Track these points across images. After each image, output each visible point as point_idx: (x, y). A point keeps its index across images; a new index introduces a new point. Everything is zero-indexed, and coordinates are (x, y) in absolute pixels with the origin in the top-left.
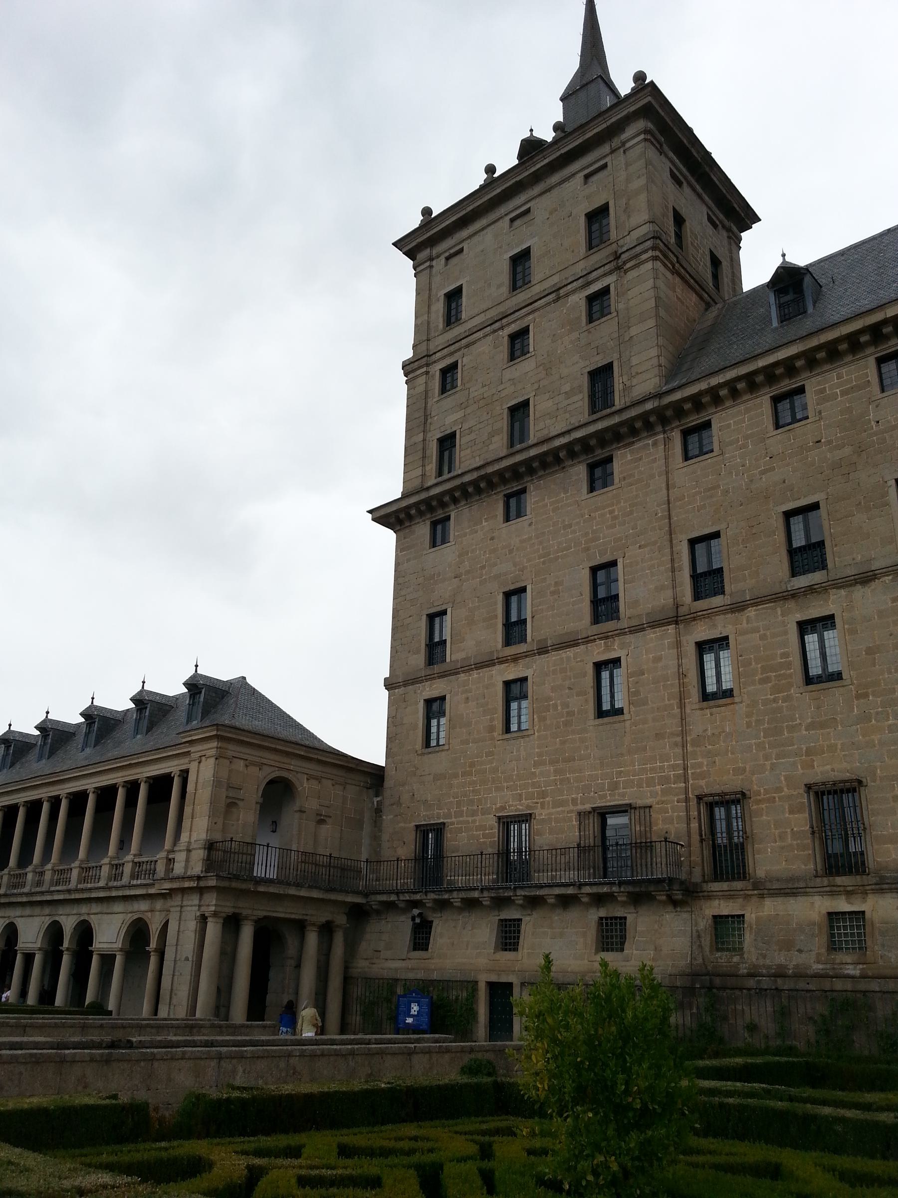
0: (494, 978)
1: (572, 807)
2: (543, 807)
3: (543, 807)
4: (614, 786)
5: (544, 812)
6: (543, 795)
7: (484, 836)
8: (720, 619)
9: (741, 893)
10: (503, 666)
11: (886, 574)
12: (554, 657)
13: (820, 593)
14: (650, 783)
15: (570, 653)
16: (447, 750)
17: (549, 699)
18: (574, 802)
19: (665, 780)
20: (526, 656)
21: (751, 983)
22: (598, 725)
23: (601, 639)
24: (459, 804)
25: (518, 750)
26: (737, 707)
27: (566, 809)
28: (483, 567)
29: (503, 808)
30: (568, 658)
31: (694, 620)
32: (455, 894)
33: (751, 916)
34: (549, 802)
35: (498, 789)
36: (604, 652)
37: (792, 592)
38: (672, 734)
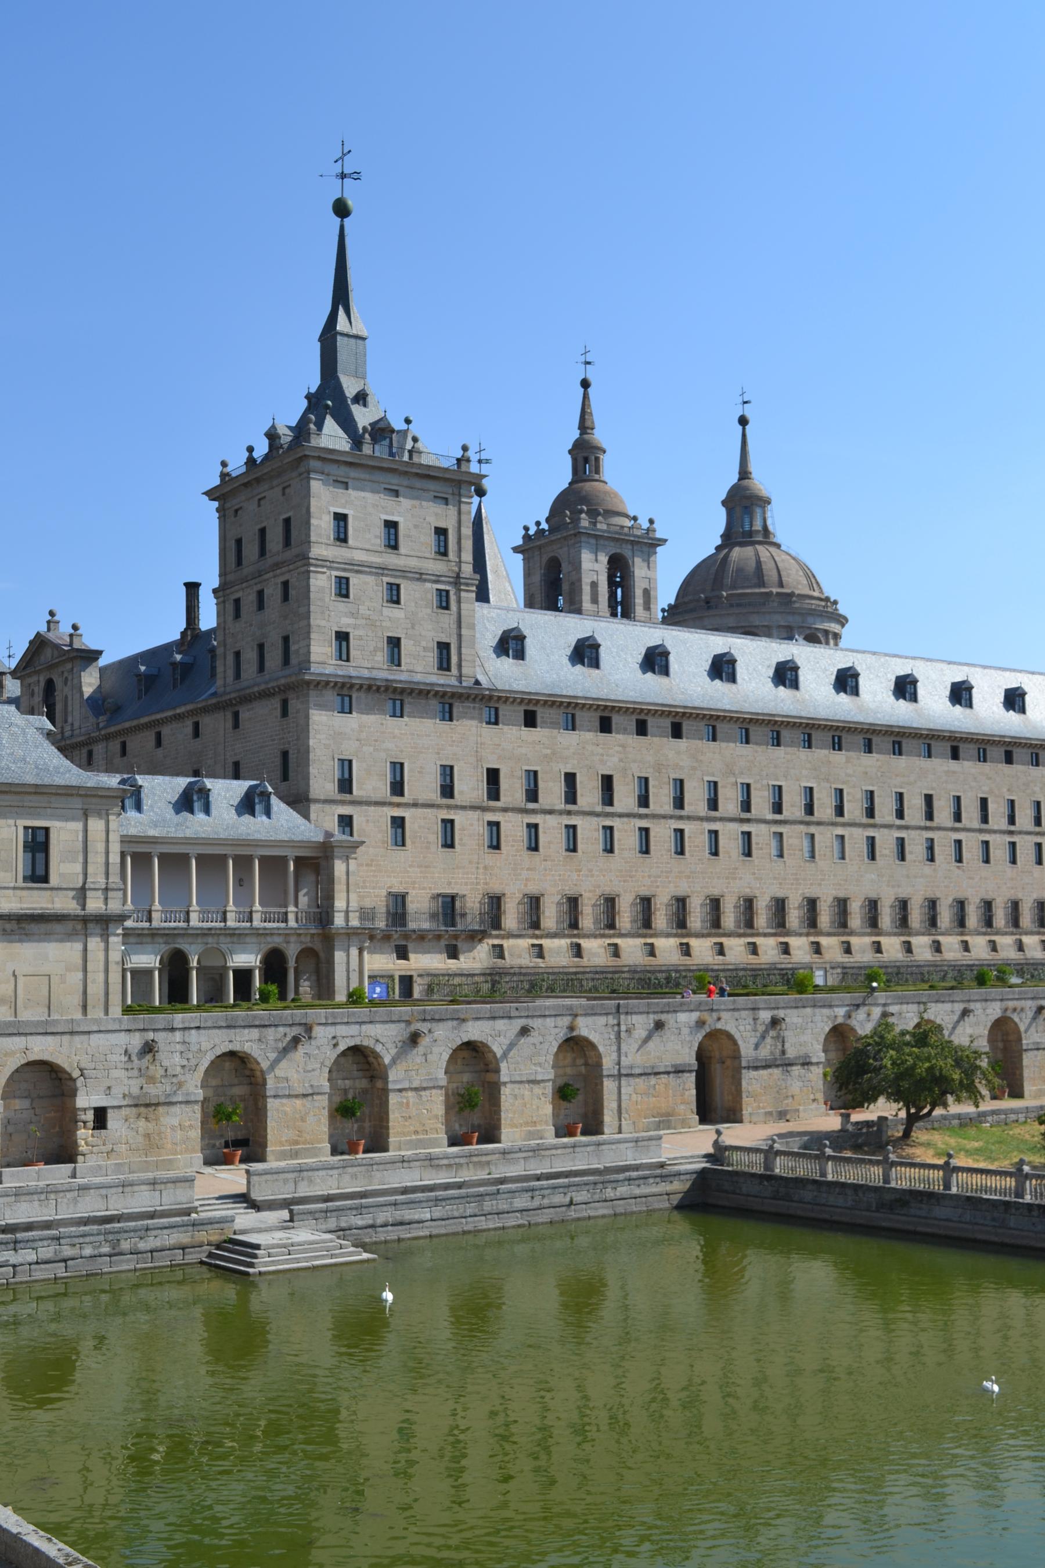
0: (403, 973)
2: (414, 888)
4: (449, 883)
6: (414, 883)
12: (420, 811)
14: (466, 884)
18: (430, 888)
19: (472, 883)
21: (512, 971)
24: (364, 882)
29: (390, 887)
33: (505, 945)
35: (388, 877)
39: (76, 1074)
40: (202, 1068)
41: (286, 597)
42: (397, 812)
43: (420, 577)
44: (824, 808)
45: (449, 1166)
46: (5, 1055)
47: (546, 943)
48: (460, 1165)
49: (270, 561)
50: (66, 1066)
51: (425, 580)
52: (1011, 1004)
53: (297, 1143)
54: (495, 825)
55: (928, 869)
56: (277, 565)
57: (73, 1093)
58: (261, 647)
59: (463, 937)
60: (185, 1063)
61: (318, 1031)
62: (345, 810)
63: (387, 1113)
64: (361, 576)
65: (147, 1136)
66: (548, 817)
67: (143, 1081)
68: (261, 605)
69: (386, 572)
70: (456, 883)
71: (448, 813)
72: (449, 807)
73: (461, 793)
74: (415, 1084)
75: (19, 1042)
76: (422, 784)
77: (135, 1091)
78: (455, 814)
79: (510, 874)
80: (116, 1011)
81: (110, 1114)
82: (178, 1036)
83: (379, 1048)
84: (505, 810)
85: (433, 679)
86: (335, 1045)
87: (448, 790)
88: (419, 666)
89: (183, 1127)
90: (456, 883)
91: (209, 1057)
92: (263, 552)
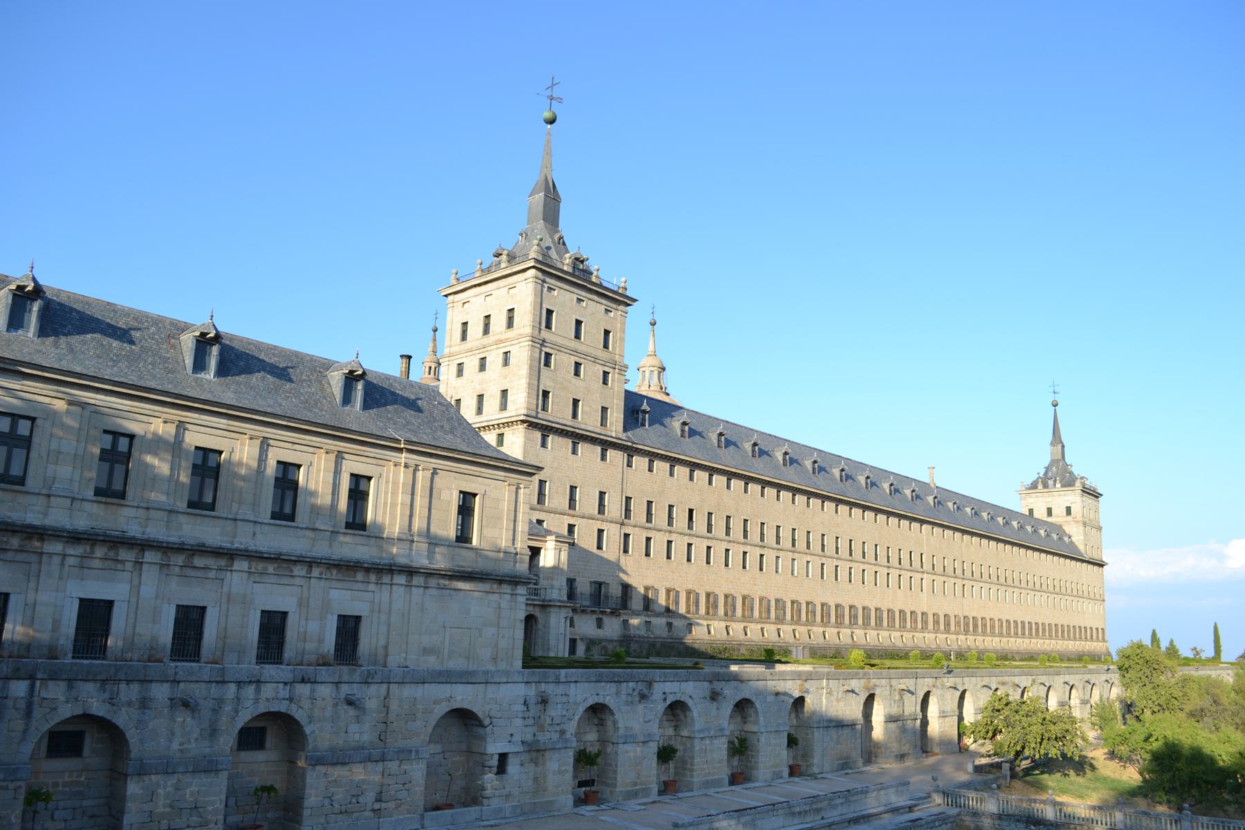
39: (487, 722)
40: (577, 718)
41: (506, 362)
43: (595, 360)
44: (801, 544)
45: (800, 813)
46: (435, 702)
47: (654, 620)
48: (806, 812)
49: (491, 338)
50: (480, 715)
52: (1000, 679)
53: (635, 784)
54: (627, 536)
55: (850, 586)
56: (501, 341)
57: (483, 739)
58: (481, 397)
60: (564, 713)
61: (658, 688)
62: (541, 516)
63: (693, 758)
65: (536, 779)
67: (535, 729)
68: (482, 367)
74: (712, 733)
75: (444, 690)
76: (587, 502)
77: (529, 738)
80: (519, 663)
81: (511, 760)
82: (560, 689)
83: (690, 703)
85: (598, 430)
86: (665, 699)
88: (588, 421)
89: (559, 771)
91: (581, 710)
92: (486, 331)
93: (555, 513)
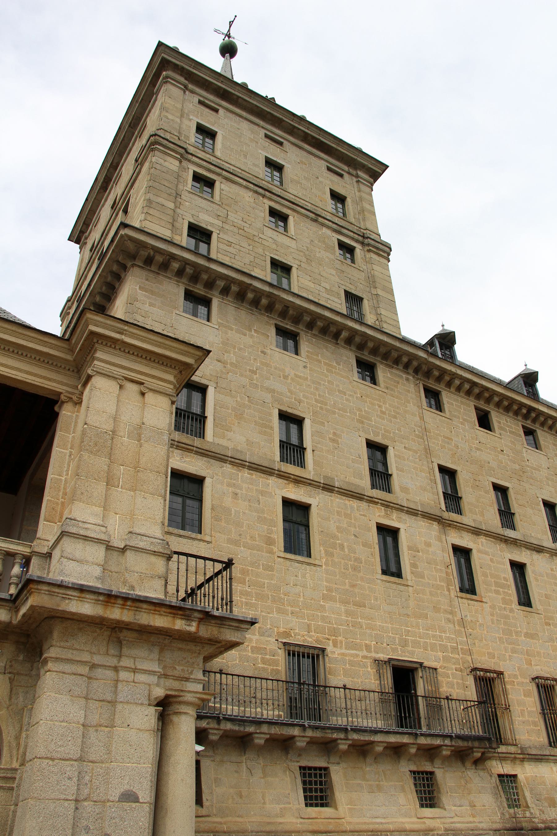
1: (365, 653)
3: (335, 645)
5: (338, 651)
7: (264, 661)
8: (465, 534)
9: (513, 756)
10: (280, 481)
11: (547, 552)
13: (517, 546)
14: (433, 648)
15: (355, 503)
16: (209, 542)
17: (335, 537)
19: (444, 649)
20: (310, 484)
22: (386, 581)
23: (382, 505)
25: (304, 576)
26: (484, 605)
27: (360, 654)
28: (254, 372)
29: (287, 634)
30: (352, 507)
31: (450, 526)
32: (265, 728)
33: (521, 777)
34: (341, 642)
35: (280, 611)
36: (383, 517)
37: (506, 538)
38: (446, 611)
42: (296, 494)
51: (323, 225)
59: (446, 752)
64: (233, 186)
66: (536, 556)
69: (268, 194)
70: (416, 644)
71: (387, 516)
72: (387, 505)
73: (405, 490)
78: (399, 520)
79: (500, 639)
84: (477, 532)
87: (381, 477)
90: (416, 644)
93: (239, 463)
